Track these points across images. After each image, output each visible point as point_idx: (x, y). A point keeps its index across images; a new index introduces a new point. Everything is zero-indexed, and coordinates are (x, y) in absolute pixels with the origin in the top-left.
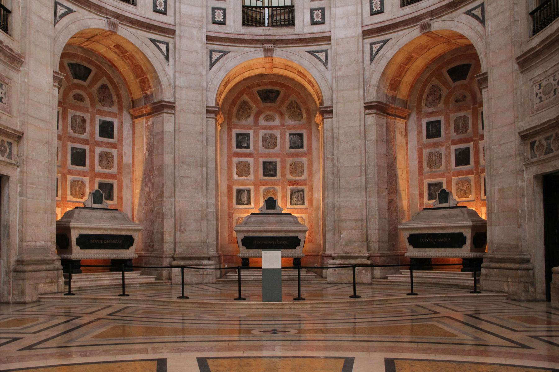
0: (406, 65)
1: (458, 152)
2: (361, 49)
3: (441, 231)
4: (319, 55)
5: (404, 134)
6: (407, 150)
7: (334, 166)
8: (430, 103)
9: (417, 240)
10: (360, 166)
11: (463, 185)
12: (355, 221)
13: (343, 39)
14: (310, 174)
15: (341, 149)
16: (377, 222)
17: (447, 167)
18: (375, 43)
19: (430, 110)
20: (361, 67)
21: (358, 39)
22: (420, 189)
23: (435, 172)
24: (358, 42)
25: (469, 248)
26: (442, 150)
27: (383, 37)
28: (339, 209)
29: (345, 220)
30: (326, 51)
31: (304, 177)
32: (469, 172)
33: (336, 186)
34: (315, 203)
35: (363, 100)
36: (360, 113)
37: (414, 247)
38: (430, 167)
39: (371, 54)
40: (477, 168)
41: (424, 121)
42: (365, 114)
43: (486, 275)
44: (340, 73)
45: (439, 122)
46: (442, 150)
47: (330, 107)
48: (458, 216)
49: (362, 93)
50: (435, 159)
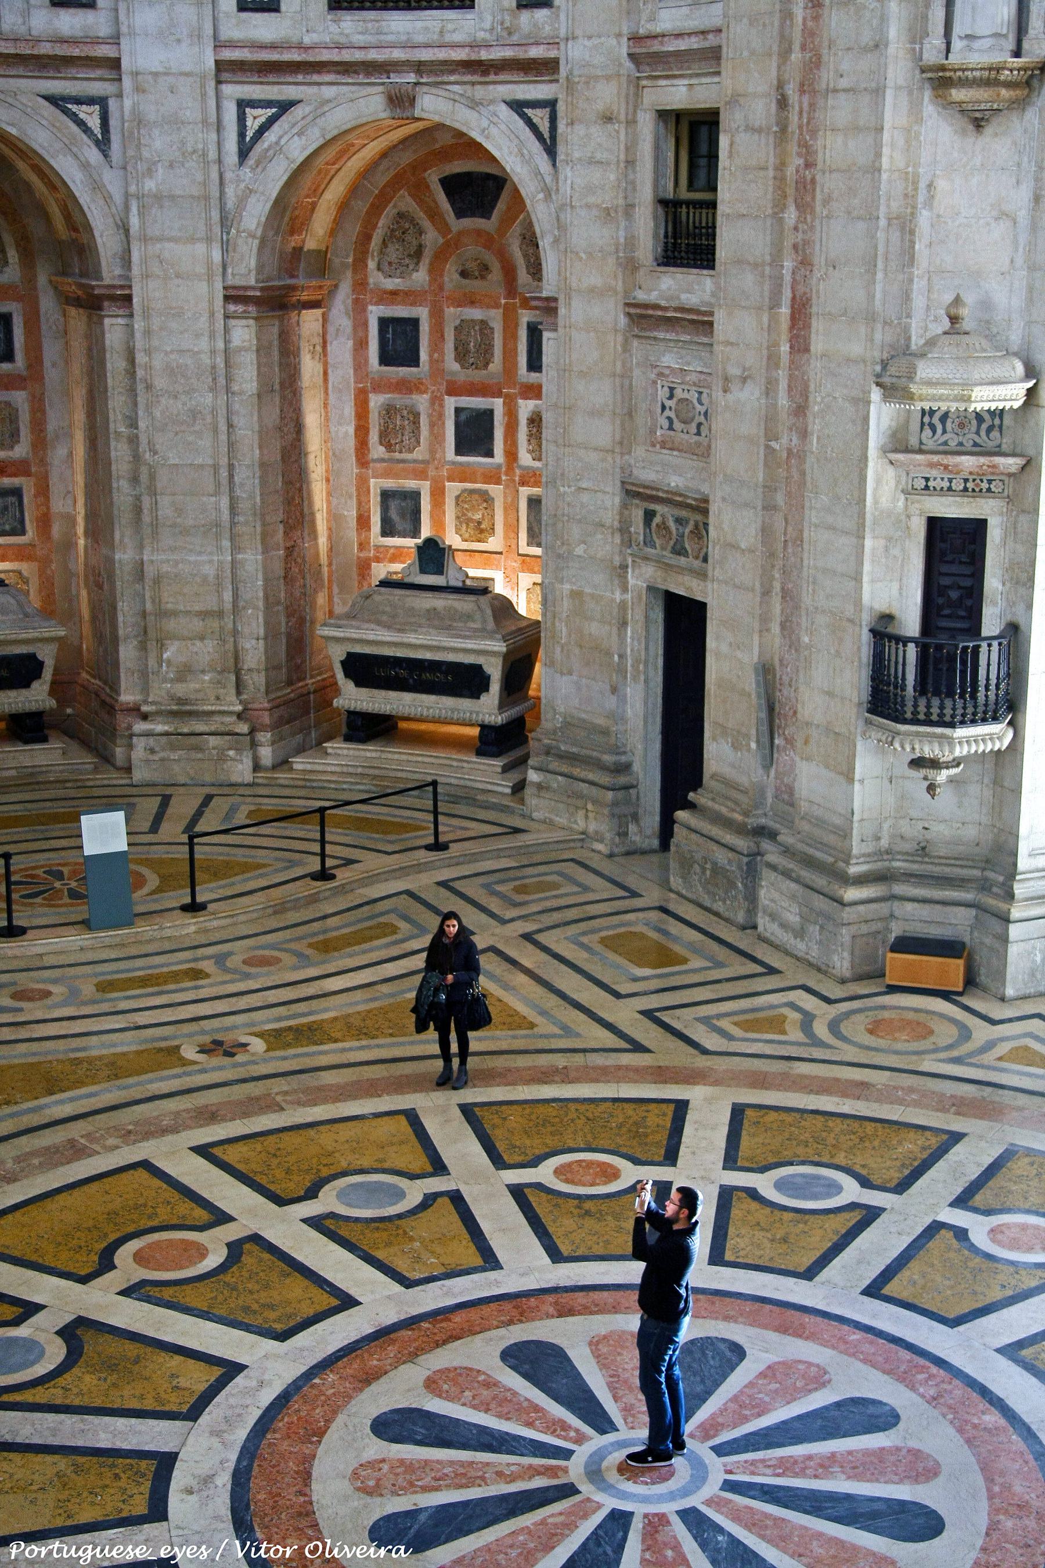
0: (334, 164)
1: (463, 417)
2: (213, 118)
3: (428, 656)
4: (84, 112)
5: (319, 348)
6: (326, 393)
7: (136, 458)
8: (390, 264)
9: (364, 669)
10: (216, 468)
11: (473, 508)
12: (204, 615)
13: (156, 75)
14: (40, 443)
15: (157, 414)
16: (261, 620)
17: (432, 452)
18: (253, 104)
19: (391, 284)
20: (214, 175)
21: (203, 86)
22: (359, 504)
23: (403, 461)
24: (204, 95)
25: (496, 702)
26: (422, 402)
27: (276, 88)
28: (157, 581)
29: (175, 613)
30: (102, 102)
31: (20, 451)
32: (493, 478)
33: (146, 518)
34: (56, 531)
35: (219, 278)
36: (212, 314)
37: (358, 684)
38: (389, 447)
39: (242, 135)
40: (510, 469)
41: (375, 312)
42: (227, 317)
43: (540, 786)
44: (150, 185)
45: (415, 322)
46: (422, 402)
47: (122, 287)
48: (469, 617)
49: (217, 255)
50: (403, 427)
